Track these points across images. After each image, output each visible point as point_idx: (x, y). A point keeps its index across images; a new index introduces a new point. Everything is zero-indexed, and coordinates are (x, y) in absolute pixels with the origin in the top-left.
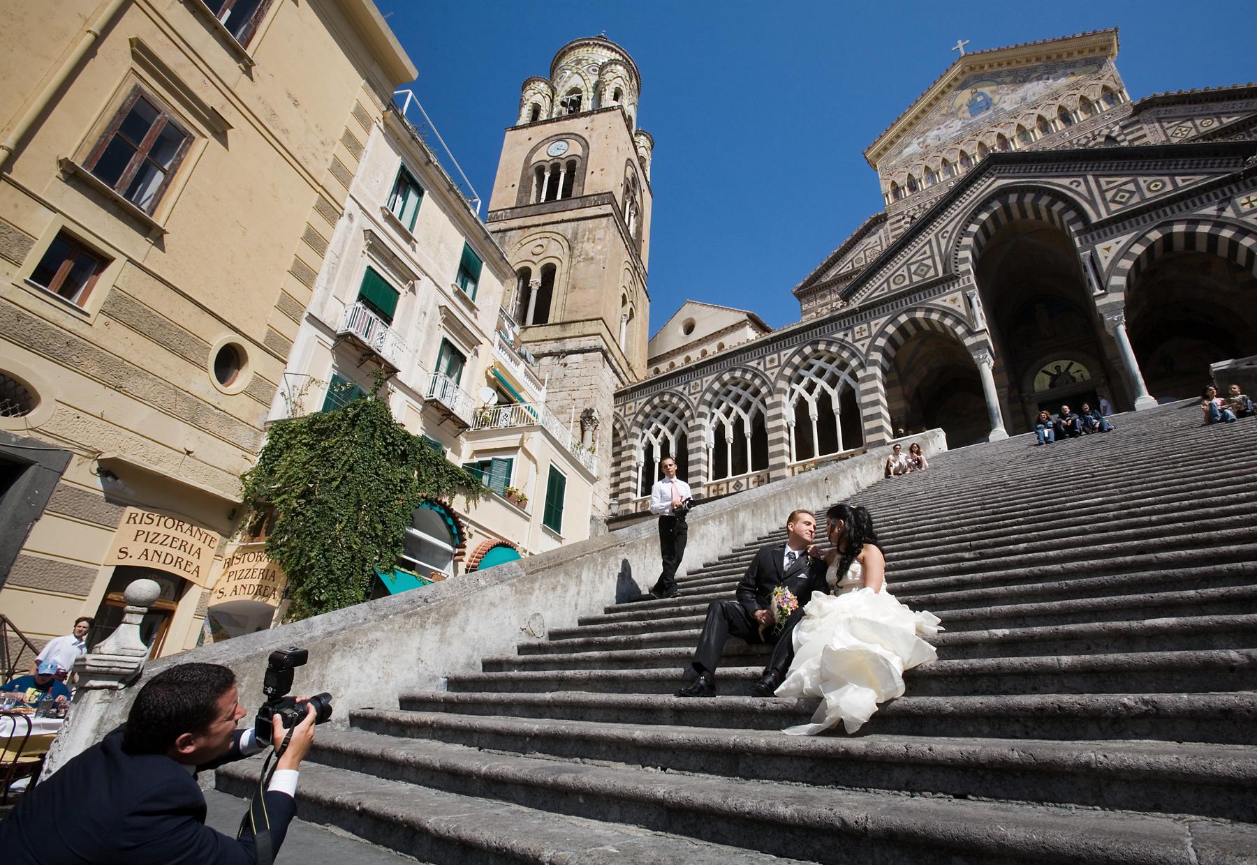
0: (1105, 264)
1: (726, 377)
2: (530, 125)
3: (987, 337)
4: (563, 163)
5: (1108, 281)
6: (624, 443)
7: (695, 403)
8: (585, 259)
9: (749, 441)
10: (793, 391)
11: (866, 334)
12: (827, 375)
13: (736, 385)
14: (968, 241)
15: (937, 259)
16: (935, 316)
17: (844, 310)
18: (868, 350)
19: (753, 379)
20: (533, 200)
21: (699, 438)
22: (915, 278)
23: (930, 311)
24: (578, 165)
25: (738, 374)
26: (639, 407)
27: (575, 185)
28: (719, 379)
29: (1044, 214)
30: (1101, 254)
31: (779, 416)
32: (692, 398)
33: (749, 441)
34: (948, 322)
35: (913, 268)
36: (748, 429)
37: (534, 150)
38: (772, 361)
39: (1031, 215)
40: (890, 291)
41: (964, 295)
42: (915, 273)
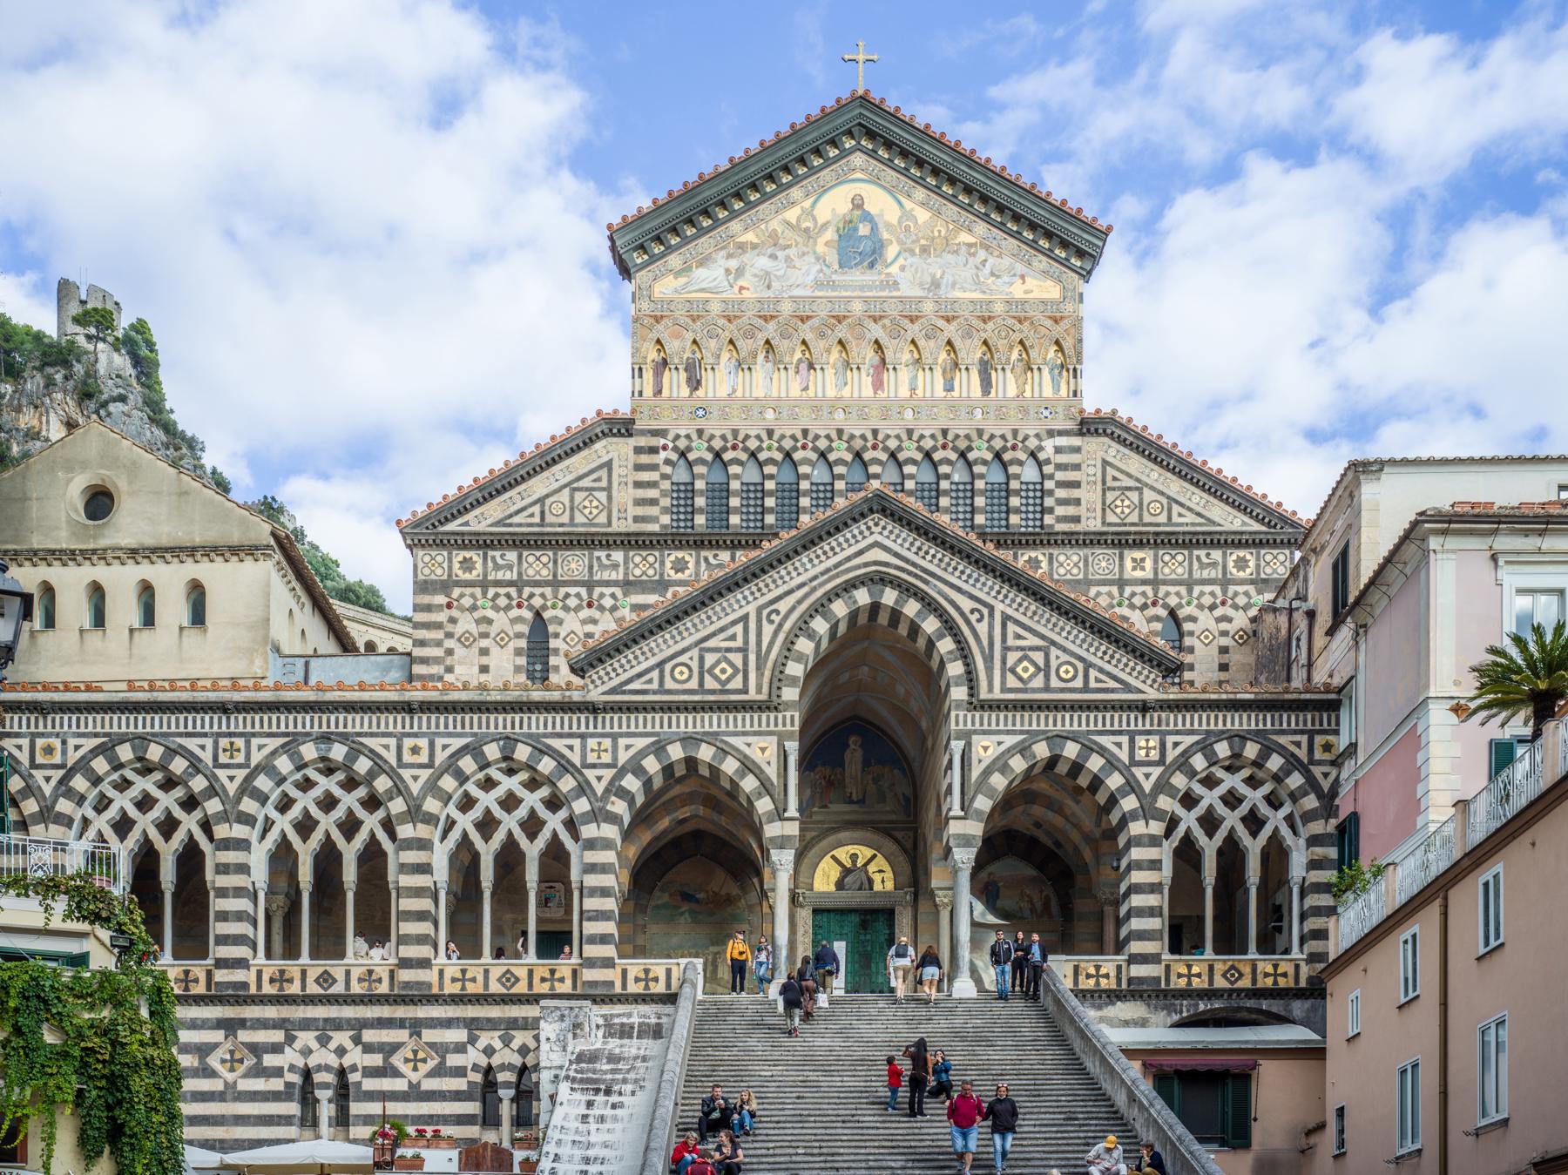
0: (976, 773)
3: (793, 829)
5: (973, 799)
10: (451, 824)
11: (606, 758)
12: (522, 812)
14: (805, 646)
15: (752, 657)
16: (730, 766)
17: (576, 696)
18: (607, 791)
22: (710, 683)
23: (723, 752)
29: (921, 642)
30: (977, 751)
31: (425, 869)
33: (350, 896)
34: (749, 784)
35: (710, 659)
36: (350, 874)
39: (903, 630)
40: (662, 690)
41: (781, 746)
42: (710, 671)
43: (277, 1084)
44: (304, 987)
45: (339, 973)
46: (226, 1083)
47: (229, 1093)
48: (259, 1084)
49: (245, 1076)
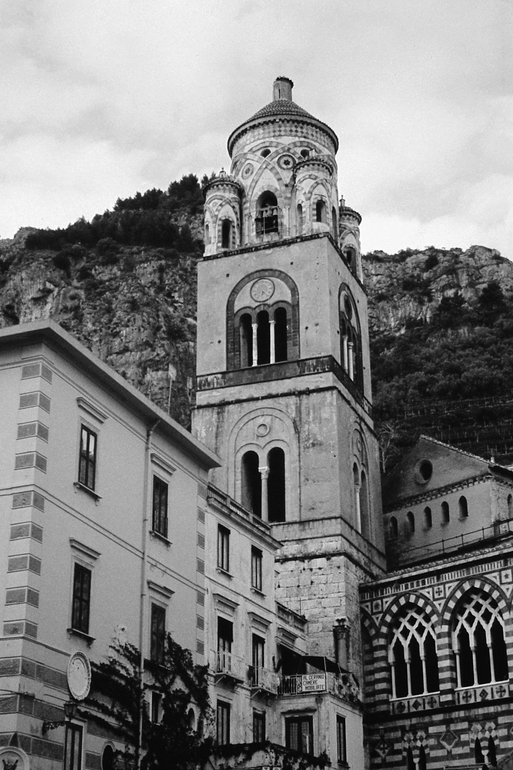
1: (467, 586)
2: (226, 254)
4: (271, 311)
6: (375, 643)
7: (440, 609)
8: (313, 445)
9: (491, 651)
13: (476, 594)
19: (491, 591)
20: (243, 365)
21: (450, 646)
24: (289, 316)
25: (477, 584)
26: (386, 606)
27: (289, 343)
28: (459, 587)
32: (436, 603)
33: (491, 651)
36: (489, 641)
37: (235, 291)
38: (507, 576)
43: (466, 750)
44: (476, 700)
45: (489, 691)
46: (448, 751)
47: (450, 756)
48: (459, 750)
49: (453, 747)
